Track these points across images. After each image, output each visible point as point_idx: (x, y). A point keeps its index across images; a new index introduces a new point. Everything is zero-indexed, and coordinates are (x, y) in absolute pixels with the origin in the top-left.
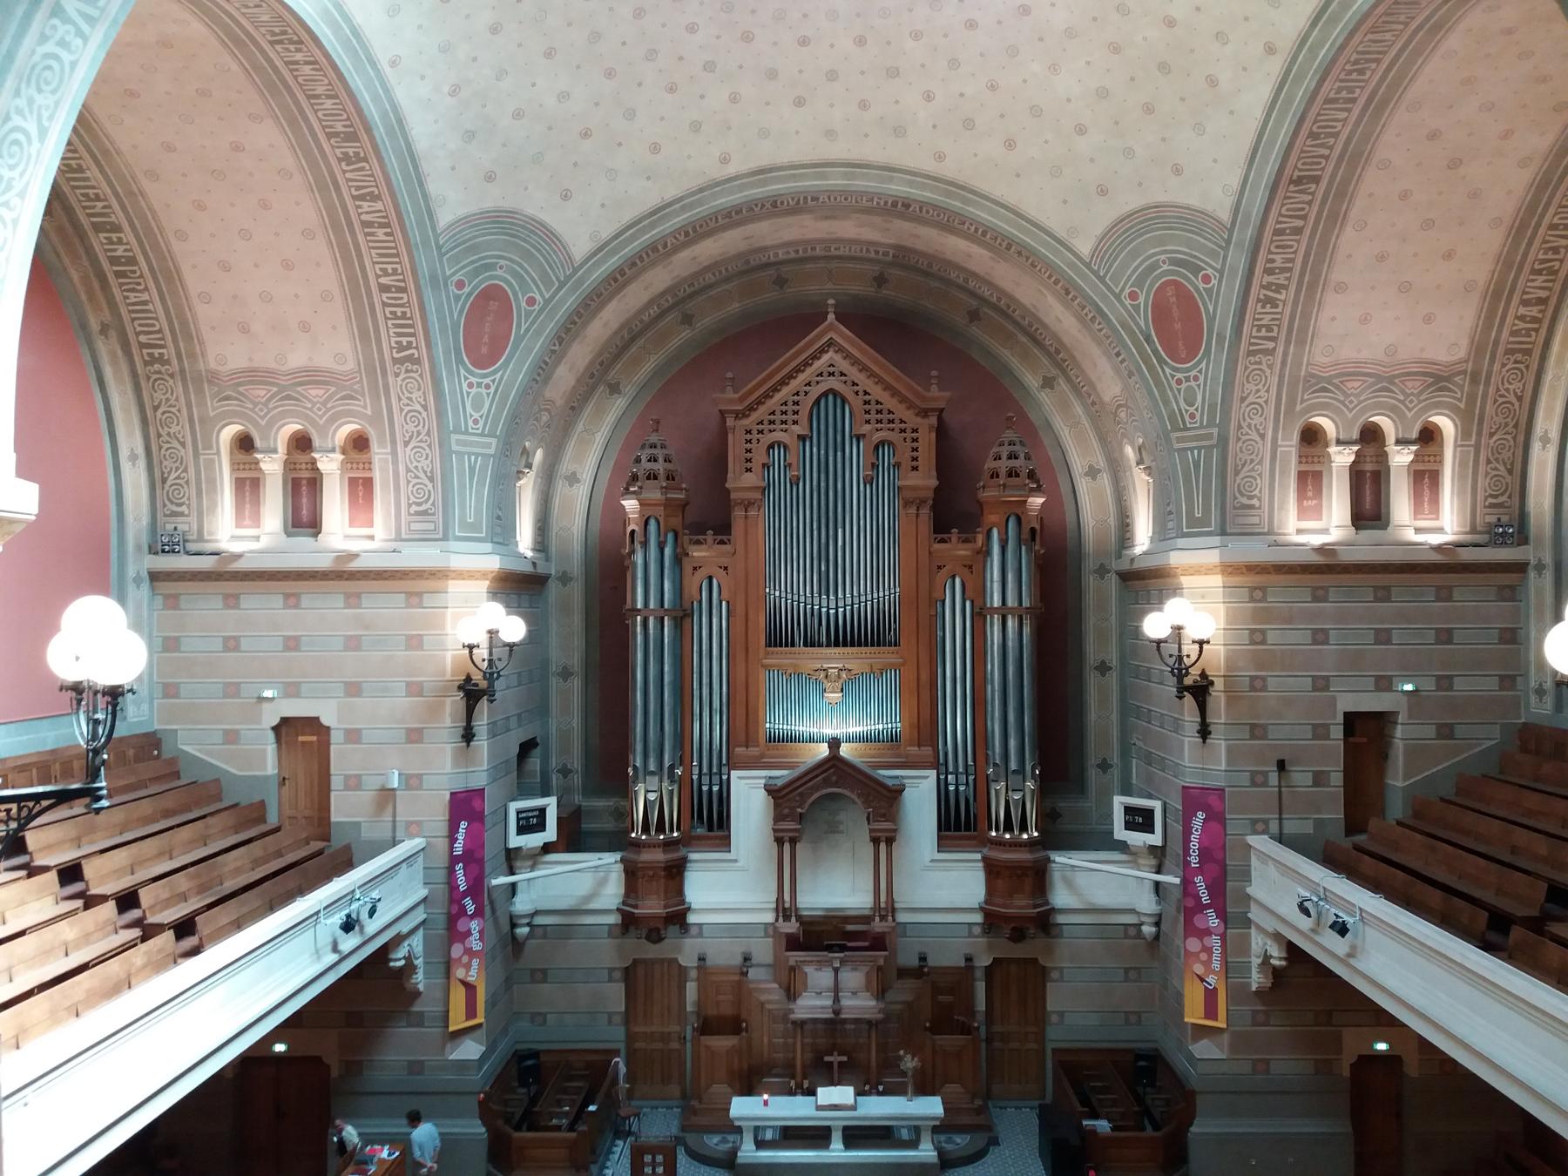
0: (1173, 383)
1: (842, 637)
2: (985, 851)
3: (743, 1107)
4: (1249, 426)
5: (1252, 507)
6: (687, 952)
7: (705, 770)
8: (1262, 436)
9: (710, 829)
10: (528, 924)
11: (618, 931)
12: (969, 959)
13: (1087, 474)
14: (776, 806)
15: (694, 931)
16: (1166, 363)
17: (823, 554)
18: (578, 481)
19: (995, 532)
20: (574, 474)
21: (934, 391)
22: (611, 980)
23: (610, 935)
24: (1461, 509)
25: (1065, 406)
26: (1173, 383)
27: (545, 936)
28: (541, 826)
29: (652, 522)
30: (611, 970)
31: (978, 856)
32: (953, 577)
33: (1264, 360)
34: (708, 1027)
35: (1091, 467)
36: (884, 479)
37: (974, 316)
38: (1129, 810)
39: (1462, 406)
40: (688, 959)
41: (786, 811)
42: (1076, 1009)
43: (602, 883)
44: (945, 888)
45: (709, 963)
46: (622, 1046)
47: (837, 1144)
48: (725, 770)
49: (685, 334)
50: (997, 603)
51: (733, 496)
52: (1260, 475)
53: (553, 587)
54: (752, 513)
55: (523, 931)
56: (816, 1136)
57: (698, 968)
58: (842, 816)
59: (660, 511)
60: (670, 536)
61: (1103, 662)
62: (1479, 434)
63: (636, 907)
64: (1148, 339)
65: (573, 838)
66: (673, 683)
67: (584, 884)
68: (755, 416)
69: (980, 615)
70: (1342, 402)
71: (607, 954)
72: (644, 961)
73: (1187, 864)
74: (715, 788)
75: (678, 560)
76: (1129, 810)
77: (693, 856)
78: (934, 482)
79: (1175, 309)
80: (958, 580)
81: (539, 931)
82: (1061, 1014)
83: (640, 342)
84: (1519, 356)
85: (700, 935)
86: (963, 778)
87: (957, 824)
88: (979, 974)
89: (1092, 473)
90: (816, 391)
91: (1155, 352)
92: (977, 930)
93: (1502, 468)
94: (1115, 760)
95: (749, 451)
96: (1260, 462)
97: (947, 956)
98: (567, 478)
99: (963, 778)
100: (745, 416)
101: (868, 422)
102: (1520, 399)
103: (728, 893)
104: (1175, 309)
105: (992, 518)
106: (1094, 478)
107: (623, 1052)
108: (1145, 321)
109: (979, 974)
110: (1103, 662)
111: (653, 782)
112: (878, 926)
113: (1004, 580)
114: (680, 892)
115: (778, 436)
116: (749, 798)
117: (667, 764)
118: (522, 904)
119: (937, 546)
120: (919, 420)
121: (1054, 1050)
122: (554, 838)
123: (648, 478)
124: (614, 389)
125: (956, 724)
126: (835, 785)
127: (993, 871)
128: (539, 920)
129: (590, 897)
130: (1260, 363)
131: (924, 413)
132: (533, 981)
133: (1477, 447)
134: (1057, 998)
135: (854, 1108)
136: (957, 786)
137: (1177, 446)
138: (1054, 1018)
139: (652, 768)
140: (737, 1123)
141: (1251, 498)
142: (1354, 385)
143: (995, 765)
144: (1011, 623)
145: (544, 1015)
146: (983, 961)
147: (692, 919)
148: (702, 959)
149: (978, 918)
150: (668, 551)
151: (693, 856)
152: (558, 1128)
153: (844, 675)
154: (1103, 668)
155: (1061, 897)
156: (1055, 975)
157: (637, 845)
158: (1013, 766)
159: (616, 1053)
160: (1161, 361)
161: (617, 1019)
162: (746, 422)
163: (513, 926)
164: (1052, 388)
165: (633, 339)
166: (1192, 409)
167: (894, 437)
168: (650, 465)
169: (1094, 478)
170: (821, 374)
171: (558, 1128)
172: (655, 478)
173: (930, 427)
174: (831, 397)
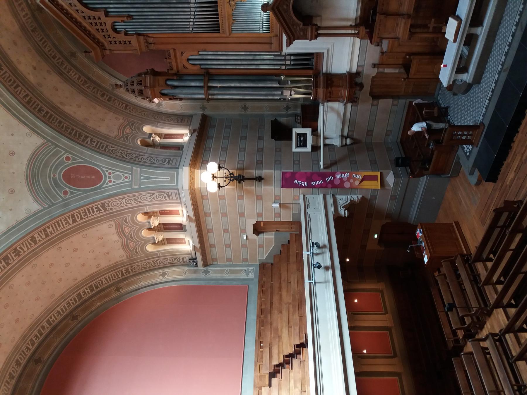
8: (157, 260)
39: (130, 215)
70: (139, 246)
93: (152, 197)
102: (123, 199)
130: (132, 270)
133: (146, 205)
141: (180, 259)
142: (131, 245)
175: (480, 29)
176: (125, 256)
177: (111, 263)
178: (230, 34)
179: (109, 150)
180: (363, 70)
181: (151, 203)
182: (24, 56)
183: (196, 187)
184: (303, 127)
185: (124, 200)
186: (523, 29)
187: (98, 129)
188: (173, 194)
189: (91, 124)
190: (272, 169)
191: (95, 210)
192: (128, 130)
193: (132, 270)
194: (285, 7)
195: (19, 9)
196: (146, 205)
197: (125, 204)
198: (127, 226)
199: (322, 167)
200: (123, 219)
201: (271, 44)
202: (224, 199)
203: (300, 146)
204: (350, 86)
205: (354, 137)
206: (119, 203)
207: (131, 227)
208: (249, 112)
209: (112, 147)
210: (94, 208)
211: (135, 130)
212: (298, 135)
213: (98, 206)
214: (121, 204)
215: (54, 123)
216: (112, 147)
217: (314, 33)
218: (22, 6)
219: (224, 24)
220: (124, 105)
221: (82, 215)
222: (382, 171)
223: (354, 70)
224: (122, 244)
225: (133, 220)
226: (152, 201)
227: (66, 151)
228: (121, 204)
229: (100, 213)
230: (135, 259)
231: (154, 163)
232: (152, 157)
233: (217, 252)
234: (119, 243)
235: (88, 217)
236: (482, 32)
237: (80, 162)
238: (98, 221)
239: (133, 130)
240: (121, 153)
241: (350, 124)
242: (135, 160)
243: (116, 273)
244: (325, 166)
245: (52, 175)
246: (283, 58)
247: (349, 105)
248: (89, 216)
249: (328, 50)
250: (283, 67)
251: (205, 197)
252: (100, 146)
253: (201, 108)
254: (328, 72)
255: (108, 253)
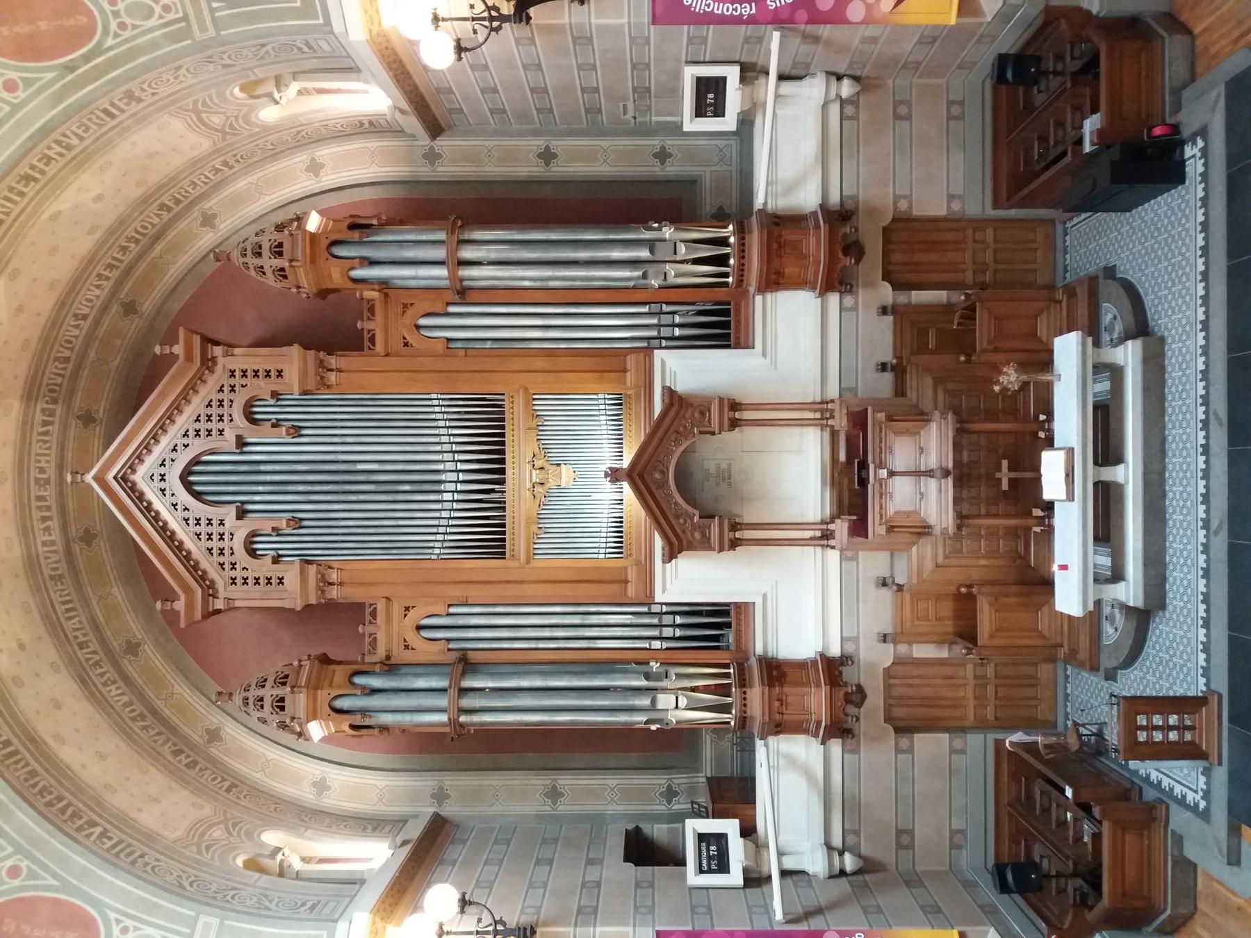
0: (127, 34)
1: (494, 465)
2: (752, 290)
3: (1069, 598)
6: (875, 657)
7: (655, 633)
9: (728, 625)
10: (841, 854)
11: (851, 743)
12: (884, 311)
13: (317, 175)
14: (691, 547)
15: (850, 648)
16: (99, 44)
17: (389, 488)
18: (323, 780)
19: (358, 273)
20: (315, 784)
21: (178, 349)
22: (910, 750)
23: (856, 751)
25: (237, 201)
26: (127, 34)
27: (857, 833)
28: (720, 840)
29: (340, 703)
30: (898, 751)
31: (759, 298)
32: (418, 327)
34: (967, 635)
35: (307, 170)
36: (293, 414)
37: (130, 308)
38: (700, 112)
40: (885, 656)
41: (697, 535)
42: (943, 177)
43: (792, 761)
44: (799, 340)
45: (889, 630)
46: (992, 737)
47: (1118, 474)
48: (656, 609)
49: (148, 649)
50: (442, 272)
51: (313, 601)
53: (450, 810)
54: (334, 576)
55: (849, 862)
56: (1106, 502)
57: (895, 642)
58: (711, 466)
59: (323, 696)
60: (359, 680)
61: (540, 156)
63: (819, 723)
64: (70, 68)
65: (734, 794)
66: (544, 674)
67: (794, 783)
68: (213, 574)
69: (463, 293)
71: (878, 753)
72: (888, 708)
73: (752, 20)
74: (679, 620)
75: (390, 667)
76: (700, 112)
77: (759, 649)
78: (295, 350)
79: (18, 29)
80: (423, 322)
81: (851, 840)
82: (951, 197)
83: (159, 704)
85: (855, 640)
86: (666, 319)
87: (721, 327)
88: (902, 298)
89: (315, 168)
90: (183, 496)
91: (87, 58)
92: (849, 300)
94: (655, 143)
95: (257, 579)
97: (880, 337)
98: (320, 793)
99: (666, 319)
100: (212, 585)
101: (221, 432)
103: (803, 603)
104: (18, 29)
105: (336, 277)
106: (322, 166)
107: (1000, 736)
108: (46, 72)
109: (902, 298)
110: (540, 156)
111: (665, 701)
112: (841, 422)
113: (416, 261)
114: (802, 665)
115: (238, 543)
116: (692, 579)
117: (643, 683)
118: (815, 863)
119: (379, 347)
120: (219, 369)
121: (996, 206)
122: (736, 822)
123: (282, 708)
124: (214, 735)
125: (610, 326)
126: (664, 473)
127: (774, 281)
128: (837, 841)
129: (808, 775)
131: (209, 363)
132: (911, 846)
134: (932, 204)
135: (1070, 452)
136: (674, 325)
137: (211, 32)
138: (956, 206)
139: (646, 702)
140: (1091, 607)
143: (645, 276)
144: (468, 253)
145: (953, 833)
146: (886, 293)
147: (835, 651)
148: (884, 638)
149: (834, 299)
150: (376, 682)
151: (759, 649)
152: (1097, 837)
153: (539, 463)
154: (547, 156)
155: (808, 198)
156: (903, 205)
157: (743, 722)
158: (644, 254)
159: (999, 744)
160: (98, 51)
161: (958, 743)
162: (220, 584)
163: (843, 873)
164: (214, 216)
165: (155, 712)
166: (158, 9)
167: (240, 399)
168: (268, 708)
169: (322, 166)
170: (163, 490)
171: (1097, 837)
172: (282, 700)
173: (226, 355)
174: (192, 478)
175: (1121, 468)
178: (528, 562)
179: (147, 864)
180: (857, 649)
182: (8, 613)
184: (717, 814)
186: (1225, 421)
187: (134, 815)
189: (118, 801)
190: (627, 925)
192: (218, 833)
194: (657, 476)
195: (39, 526)
199: (779, 916)
201: (626, 582)
203: (710, 871)
204: (831, 695)
205: (864, 851)
208: (564, 807)
209: (157, 860)
211: (239, 835)
212: (702, 838)
215: (16, 770)
216: (157, 860)
217: (728, 535)
218: (49, 523)
219: (517, 537)
220: (227, 784)
222: (963, 929)
223: (835, 198)
231: (269, 909)
232: (266, 896)
236: (1128, 474)
237: (46, 887)
239: (230, 834)
240: (180, 877)
241: (846, 807)
242: (215, 898)
244: (789, 917)
246: (655, 621)
247: (836, 746)
249: (765, 596)
250: (656, 644)
252: (121, 851)
253: (433, 796)
254: (770, 654)
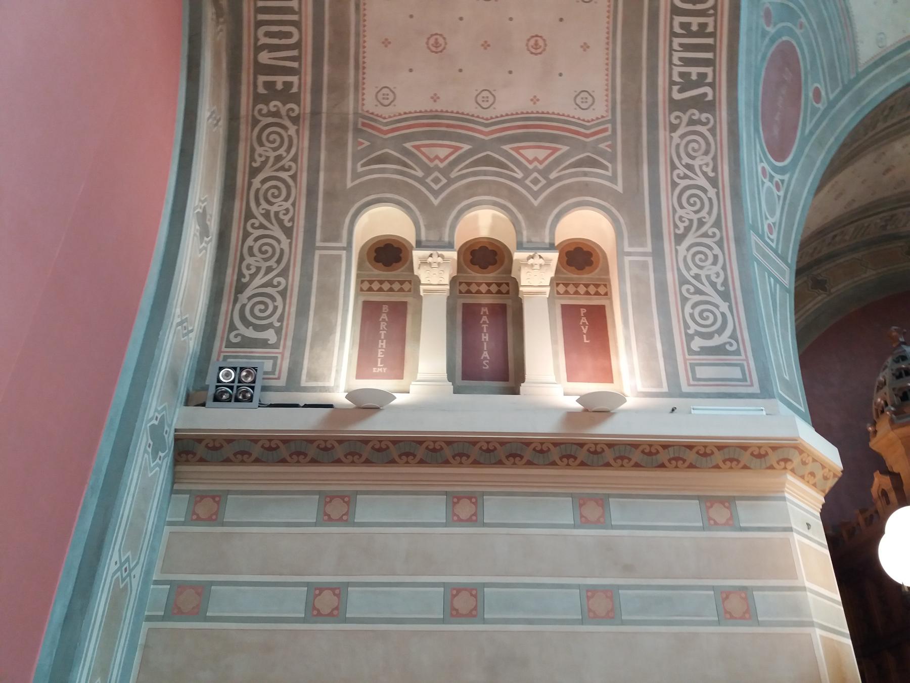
4: (267, 215)
5: (264, 344)
8: (288, 232)
24: (648, 356)
33: (283, 111)
52: (283, 293)
62: (657, 236)
70: (421, 181)
84: (696, 114)
93: (708, 289)
96: (284, 273)
102: (714, 182)
133: (658, 253)
176: (380, 110)
177: (371, 43)
181: (671, 278)
183: (790, 477)
185: (702, 182)
188: (736, 373)
191: (694, 71)
193: (277, 114)
196: (658, 253)
197: (683, 183)
198: (557, 162)
200: (602, 153)
202: (726, 616)
206: (696, 163)
207: (545, 173)
210: (709, 70)
213: (712, 85)
214: (689, 167)
221: (695, 22)
224: (465, 119)
225: (585, 189)
226: (683, 281)
227: (831, 105)
228: (689, 167)
229: (672, 83)
230: (338, 145)
233: (278, 537)
234: (470, 108)
235: (674, 34)
238: (633, 62)
243: (298, 46)
245: (803, 20)
248: (677, 41)
251: (720, 514)
255: (437, 46)
